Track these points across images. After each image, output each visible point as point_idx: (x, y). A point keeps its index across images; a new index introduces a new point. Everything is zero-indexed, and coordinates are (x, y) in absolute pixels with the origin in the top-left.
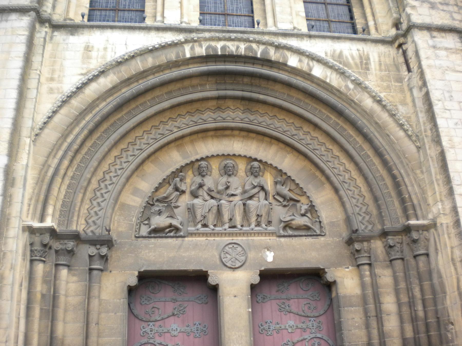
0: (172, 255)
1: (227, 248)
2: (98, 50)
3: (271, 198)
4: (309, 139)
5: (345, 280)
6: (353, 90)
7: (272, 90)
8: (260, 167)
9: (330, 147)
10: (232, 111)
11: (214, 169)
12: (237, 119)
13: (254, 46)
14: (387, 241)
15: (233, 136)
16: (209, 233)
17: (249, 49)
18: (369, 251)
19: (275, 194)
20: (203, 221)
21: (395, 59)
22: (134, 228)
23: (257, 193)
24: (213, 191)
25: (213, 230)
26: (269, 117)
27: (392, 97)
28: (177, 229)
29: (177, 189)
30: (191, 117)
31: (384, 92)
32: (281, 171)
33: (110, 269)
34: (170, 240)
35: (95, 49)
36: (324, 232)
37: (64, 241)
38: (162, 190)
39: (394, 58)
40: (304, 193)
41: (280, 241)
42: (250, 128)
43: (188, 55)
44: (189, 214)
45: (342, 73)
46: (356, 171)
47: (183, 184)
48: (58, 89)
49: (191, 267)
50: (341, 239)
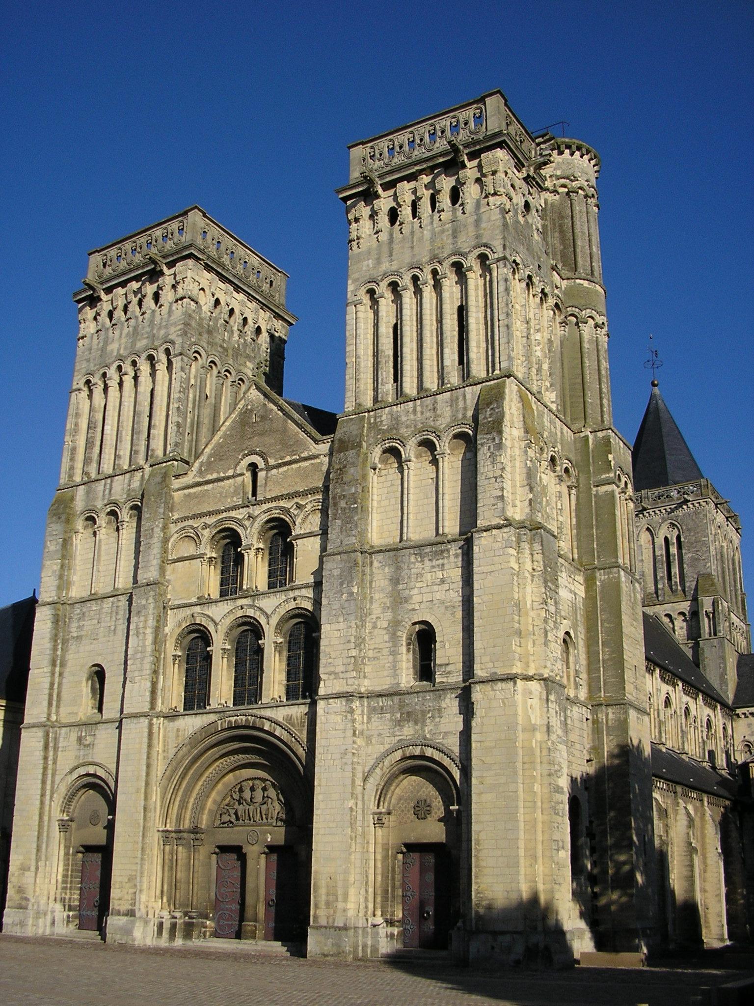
17: (247, 720)
49: (236, 844)
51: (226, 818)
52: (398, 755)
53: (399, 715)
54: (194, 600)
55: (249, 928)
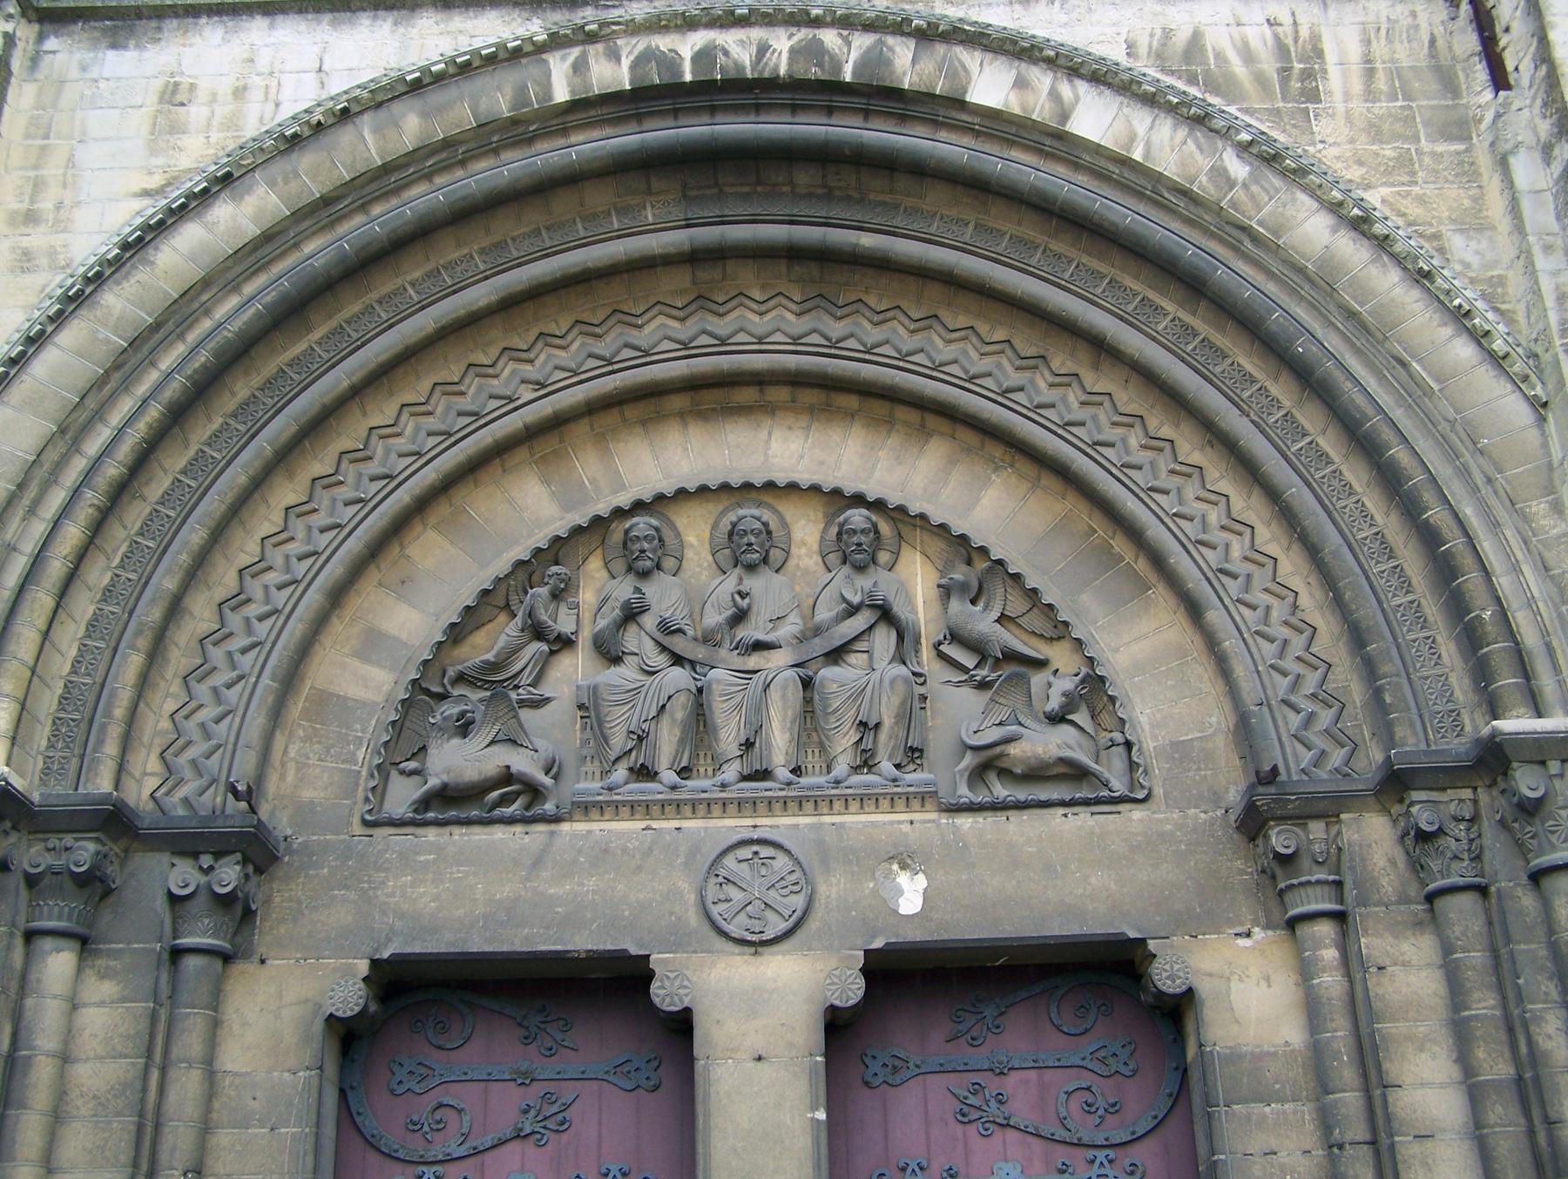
0: (505, 891)
1: (730, 861)
2: (214, 98)
3: (926, 652)
4: (1076, 405)
5: (1235, 985)
6: (1245, 186)
7: (914, 212)
8: (877, 532)
9: (1166, 431)
10: (754, 306)
11: (692, 546)
12: (778, 337)
13: (830, 38)
14: (1408, 814)
15: (770, 409)
16: (655, 802)
18: (1335, 858)
19: (941, 637)
20: (634, 753)
21: (1440, 43)
22: (361, 789)
23: (863, 633)
24: (680, 631)
25: (674, 788)
26: (906, 321)
27: (1422, 200)
28: (534, 792)
29: (537, 631)
30: (590, 340)
31: (1384, 184)
32: (963, 539)
33: (262, 950)
34: (499, 833)
35: (202, 95)
36: (1143, 787)
37: (60, 839)
38: (479, 638)
39: (1433, 42)
40: (1059, 625)
41: (956, 829)
42: (830, 370)
43: (561, 94)
44: (584, 728)
45: (1199, 120)
46: (1274, 525)
47: (563, 609)
48: (52, 253)
49: (582, 941)
50: (1220, 812)
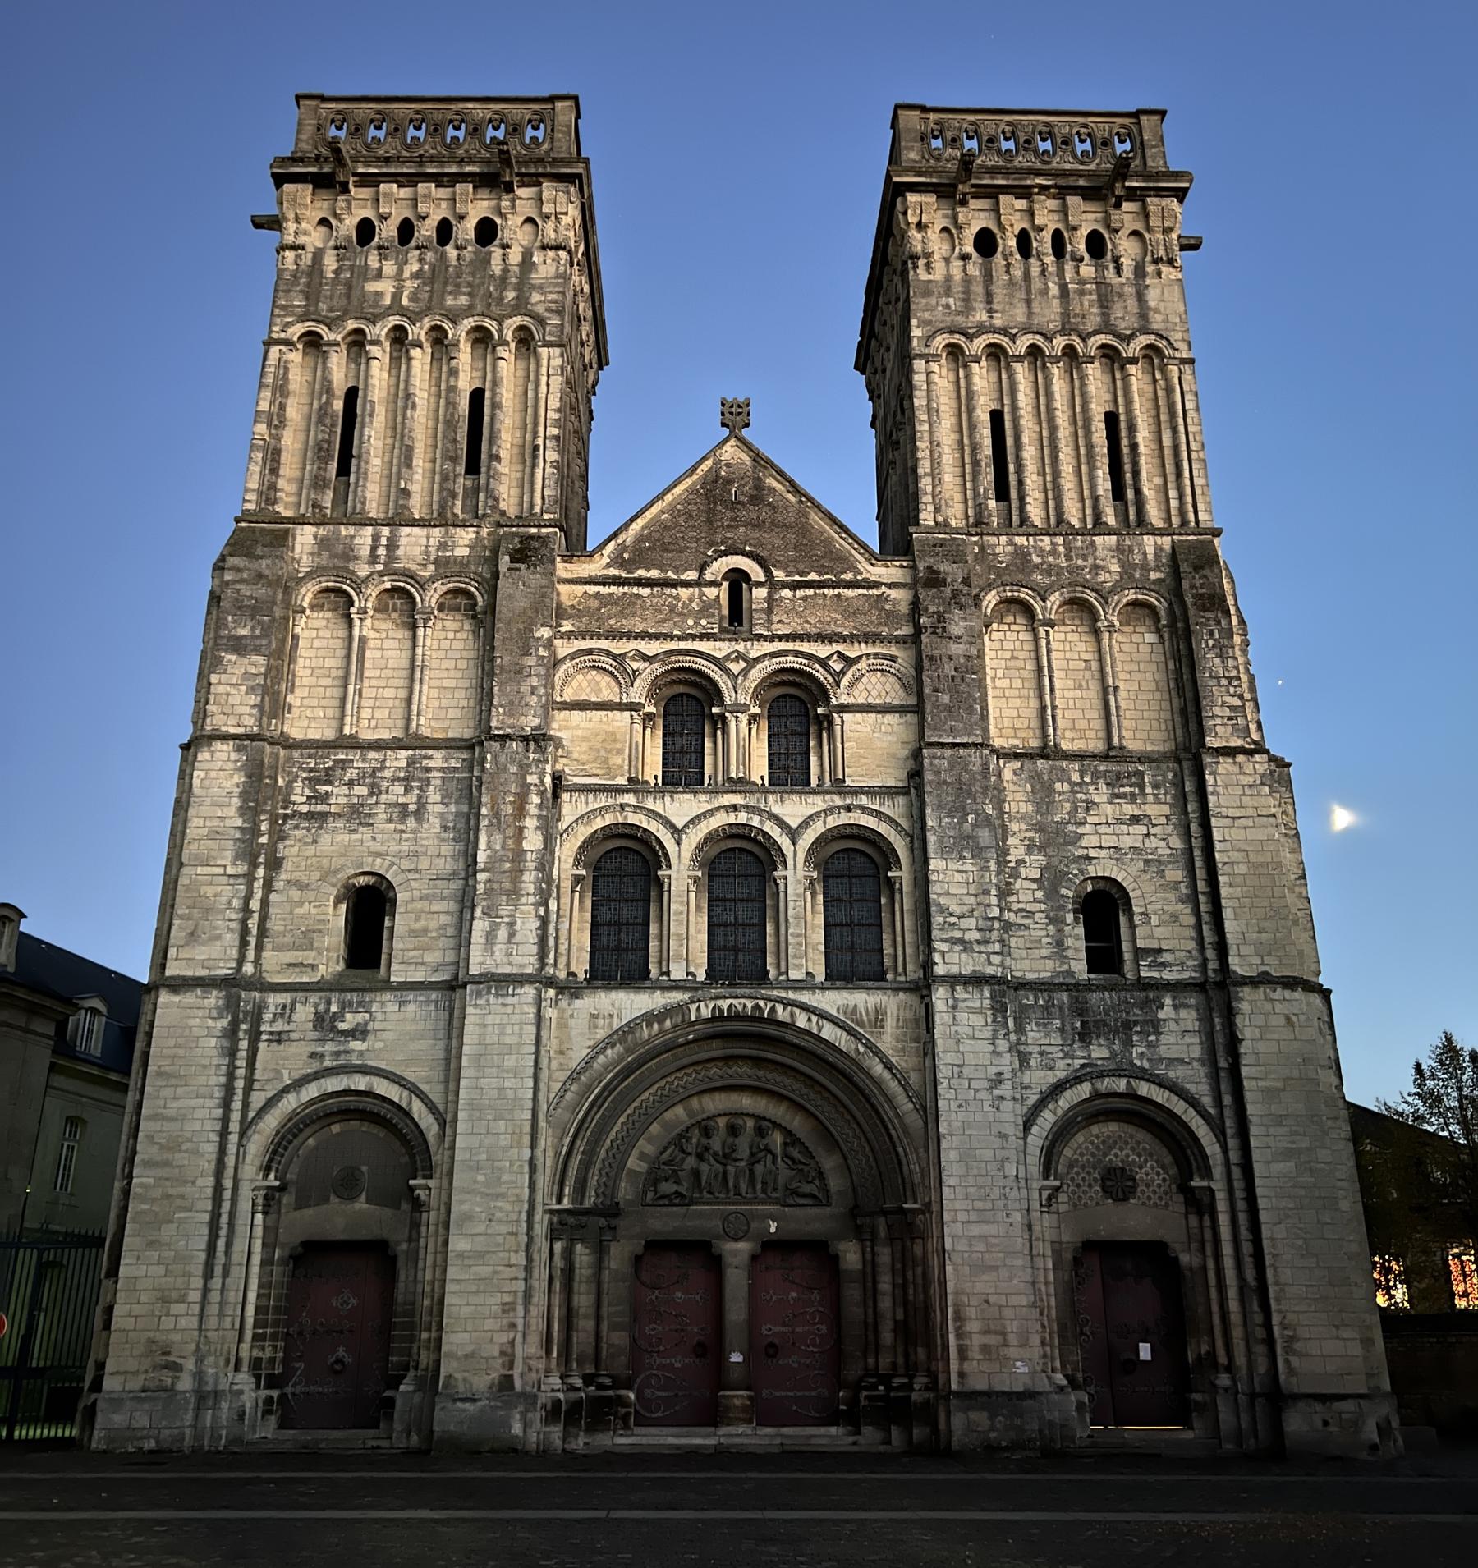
17: (757, 1006)
28: (682, 1196)
29: (683, 1151)
45: (851, 1032)
51: (667, 1187)
52: (1084, 1090)
53: (1078, 1024)
54: (622, 781)
55: (737, 1402)
